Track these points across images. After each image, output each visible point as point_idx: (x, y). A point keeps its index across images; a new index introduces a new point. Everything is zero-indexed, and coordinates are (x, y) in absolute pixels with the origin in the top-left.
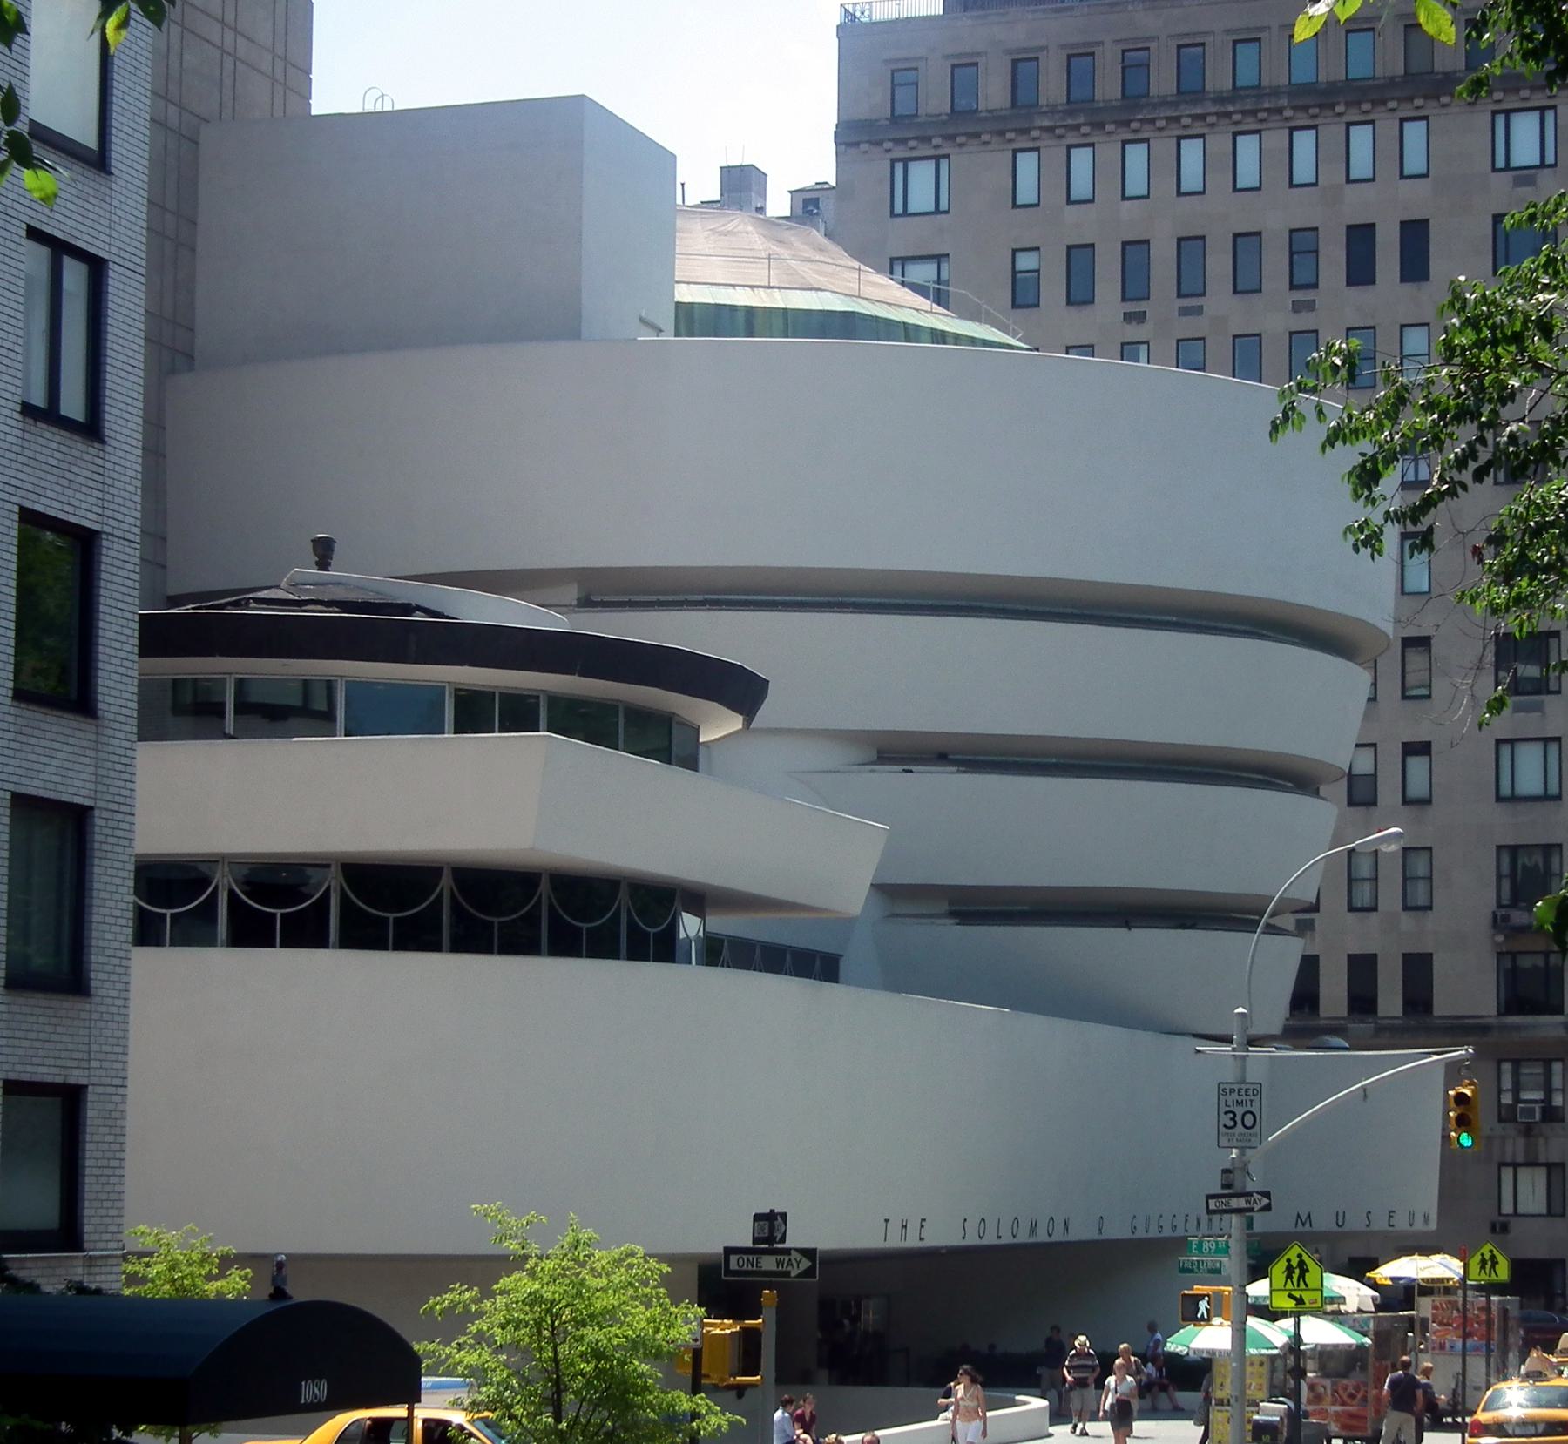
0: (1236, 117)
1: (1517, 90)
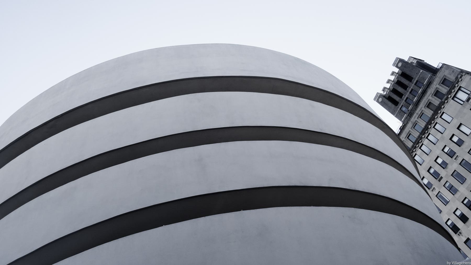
1: (451, 92)
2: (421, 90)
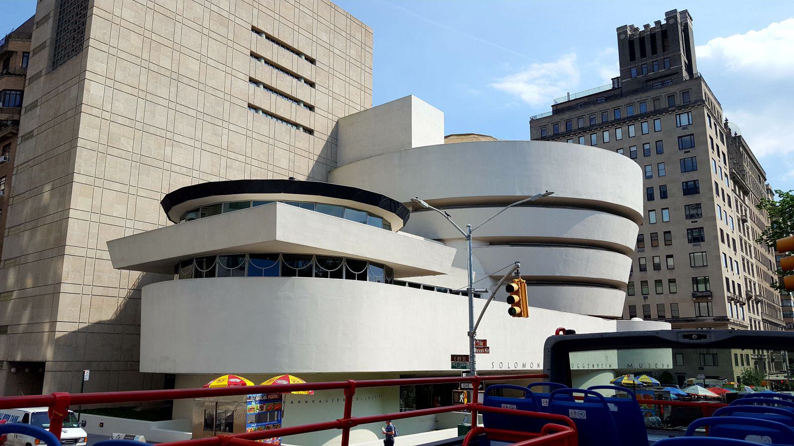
0: (615, 125)
1: (681, 109)
2: (663, 70)
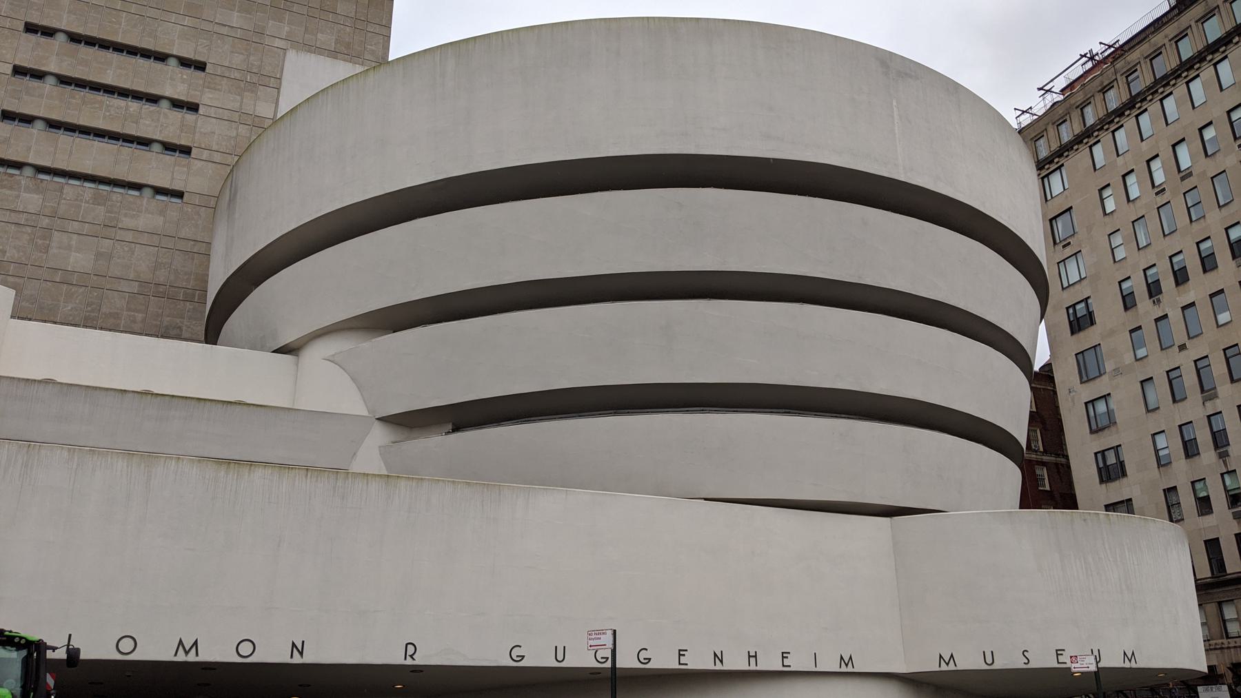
0: (1184, 75)
